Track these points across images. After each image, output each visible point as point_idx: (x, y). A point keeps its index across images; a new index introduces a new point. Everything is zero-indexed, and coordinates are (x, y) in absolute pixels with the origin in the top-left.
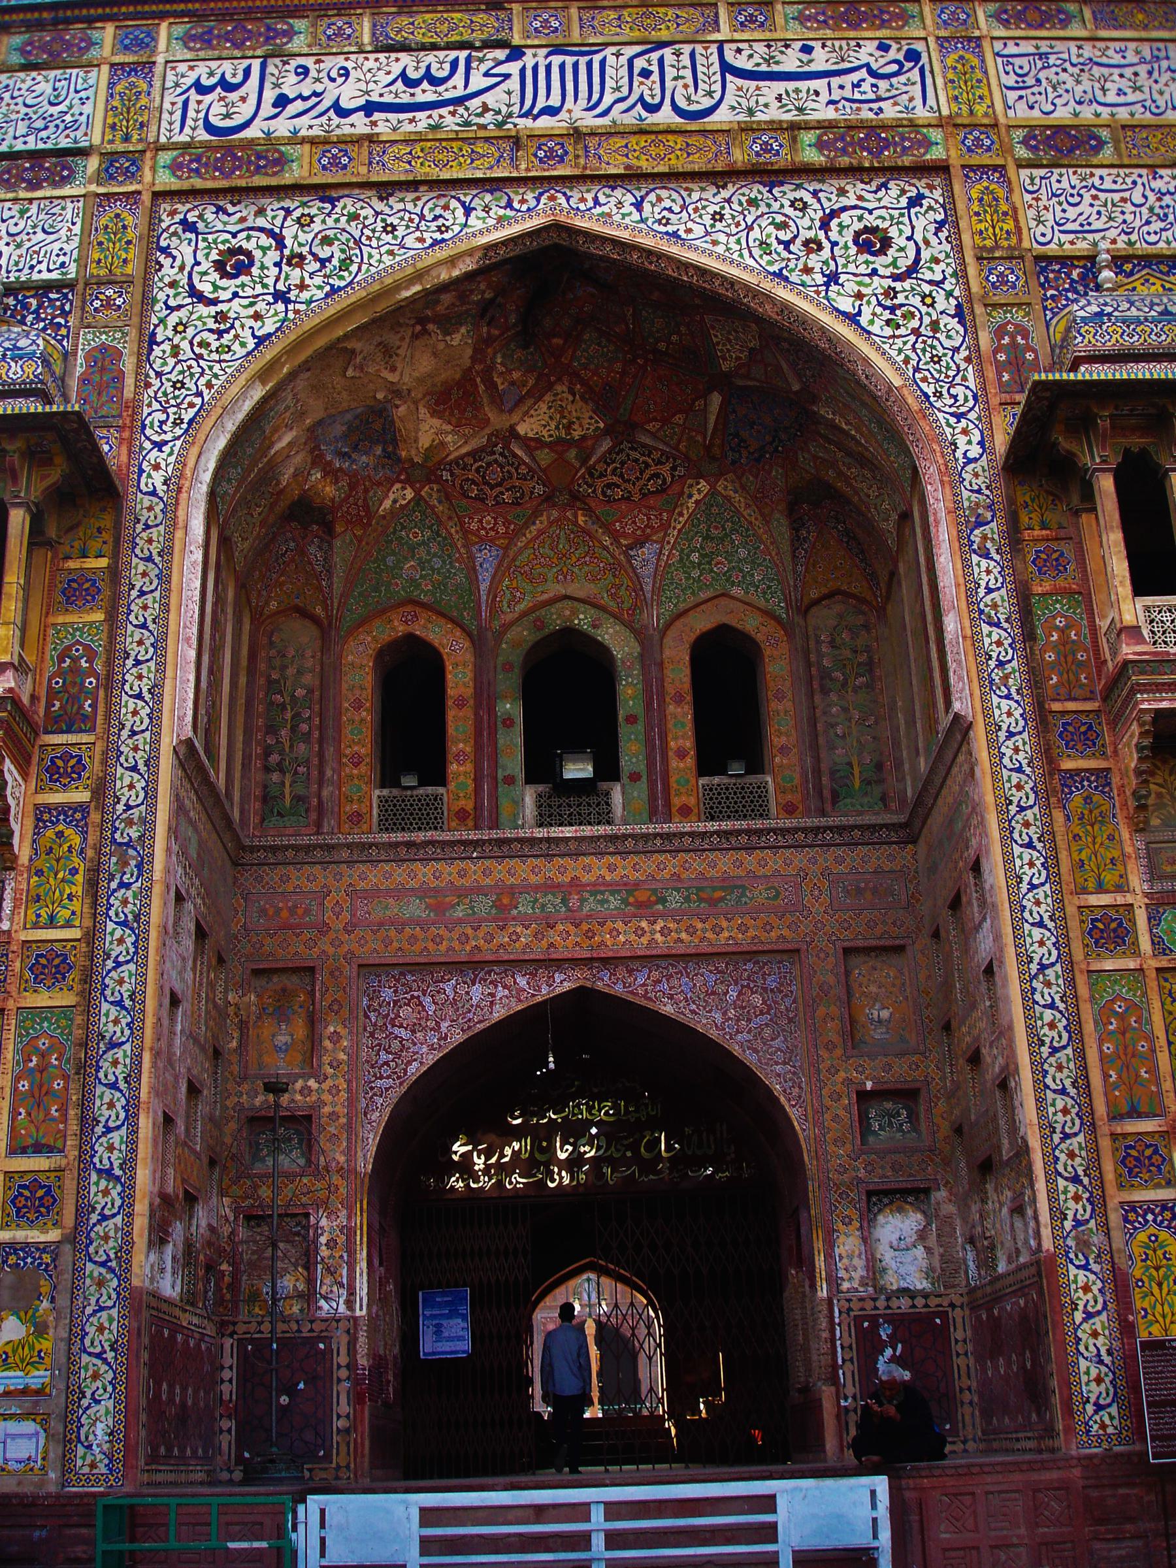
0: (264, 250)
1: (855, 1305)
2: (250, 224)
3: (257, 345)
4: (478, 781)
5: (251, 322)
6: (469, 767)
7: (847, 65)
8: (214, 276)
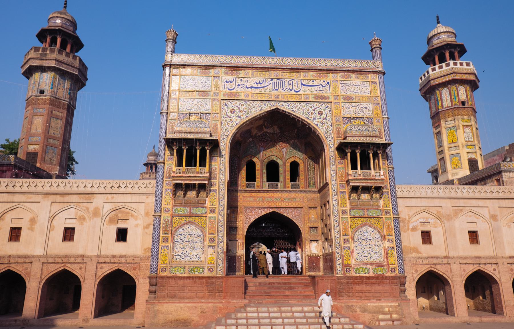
0: (237, 109)
1: (308, 255)
2: (235, 105)
4: (260, 181)
5: (235, 121)
6: (259, 179)
7: (319, 84)
8: (230, 113)
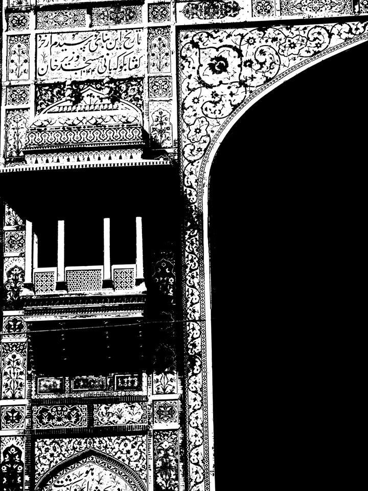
3: (234, 109)
